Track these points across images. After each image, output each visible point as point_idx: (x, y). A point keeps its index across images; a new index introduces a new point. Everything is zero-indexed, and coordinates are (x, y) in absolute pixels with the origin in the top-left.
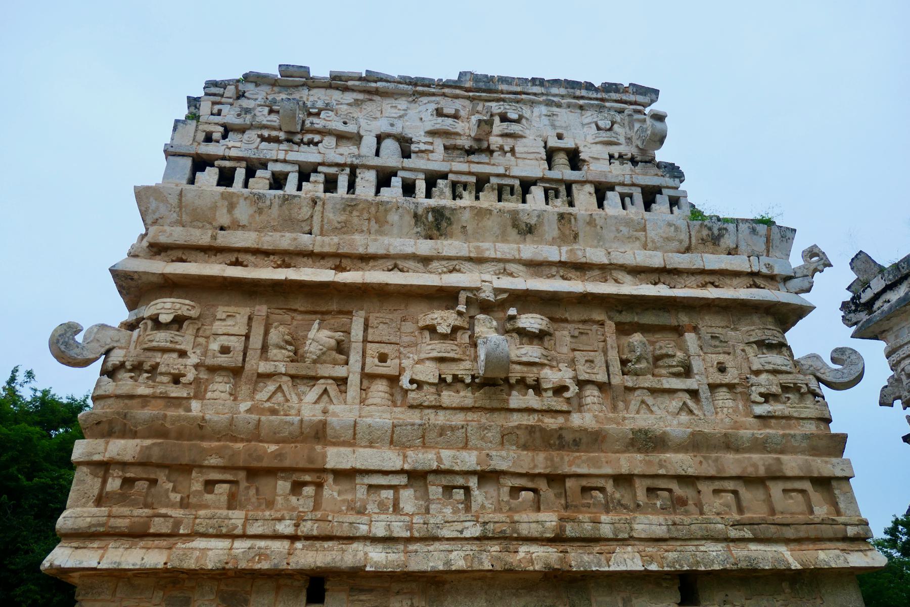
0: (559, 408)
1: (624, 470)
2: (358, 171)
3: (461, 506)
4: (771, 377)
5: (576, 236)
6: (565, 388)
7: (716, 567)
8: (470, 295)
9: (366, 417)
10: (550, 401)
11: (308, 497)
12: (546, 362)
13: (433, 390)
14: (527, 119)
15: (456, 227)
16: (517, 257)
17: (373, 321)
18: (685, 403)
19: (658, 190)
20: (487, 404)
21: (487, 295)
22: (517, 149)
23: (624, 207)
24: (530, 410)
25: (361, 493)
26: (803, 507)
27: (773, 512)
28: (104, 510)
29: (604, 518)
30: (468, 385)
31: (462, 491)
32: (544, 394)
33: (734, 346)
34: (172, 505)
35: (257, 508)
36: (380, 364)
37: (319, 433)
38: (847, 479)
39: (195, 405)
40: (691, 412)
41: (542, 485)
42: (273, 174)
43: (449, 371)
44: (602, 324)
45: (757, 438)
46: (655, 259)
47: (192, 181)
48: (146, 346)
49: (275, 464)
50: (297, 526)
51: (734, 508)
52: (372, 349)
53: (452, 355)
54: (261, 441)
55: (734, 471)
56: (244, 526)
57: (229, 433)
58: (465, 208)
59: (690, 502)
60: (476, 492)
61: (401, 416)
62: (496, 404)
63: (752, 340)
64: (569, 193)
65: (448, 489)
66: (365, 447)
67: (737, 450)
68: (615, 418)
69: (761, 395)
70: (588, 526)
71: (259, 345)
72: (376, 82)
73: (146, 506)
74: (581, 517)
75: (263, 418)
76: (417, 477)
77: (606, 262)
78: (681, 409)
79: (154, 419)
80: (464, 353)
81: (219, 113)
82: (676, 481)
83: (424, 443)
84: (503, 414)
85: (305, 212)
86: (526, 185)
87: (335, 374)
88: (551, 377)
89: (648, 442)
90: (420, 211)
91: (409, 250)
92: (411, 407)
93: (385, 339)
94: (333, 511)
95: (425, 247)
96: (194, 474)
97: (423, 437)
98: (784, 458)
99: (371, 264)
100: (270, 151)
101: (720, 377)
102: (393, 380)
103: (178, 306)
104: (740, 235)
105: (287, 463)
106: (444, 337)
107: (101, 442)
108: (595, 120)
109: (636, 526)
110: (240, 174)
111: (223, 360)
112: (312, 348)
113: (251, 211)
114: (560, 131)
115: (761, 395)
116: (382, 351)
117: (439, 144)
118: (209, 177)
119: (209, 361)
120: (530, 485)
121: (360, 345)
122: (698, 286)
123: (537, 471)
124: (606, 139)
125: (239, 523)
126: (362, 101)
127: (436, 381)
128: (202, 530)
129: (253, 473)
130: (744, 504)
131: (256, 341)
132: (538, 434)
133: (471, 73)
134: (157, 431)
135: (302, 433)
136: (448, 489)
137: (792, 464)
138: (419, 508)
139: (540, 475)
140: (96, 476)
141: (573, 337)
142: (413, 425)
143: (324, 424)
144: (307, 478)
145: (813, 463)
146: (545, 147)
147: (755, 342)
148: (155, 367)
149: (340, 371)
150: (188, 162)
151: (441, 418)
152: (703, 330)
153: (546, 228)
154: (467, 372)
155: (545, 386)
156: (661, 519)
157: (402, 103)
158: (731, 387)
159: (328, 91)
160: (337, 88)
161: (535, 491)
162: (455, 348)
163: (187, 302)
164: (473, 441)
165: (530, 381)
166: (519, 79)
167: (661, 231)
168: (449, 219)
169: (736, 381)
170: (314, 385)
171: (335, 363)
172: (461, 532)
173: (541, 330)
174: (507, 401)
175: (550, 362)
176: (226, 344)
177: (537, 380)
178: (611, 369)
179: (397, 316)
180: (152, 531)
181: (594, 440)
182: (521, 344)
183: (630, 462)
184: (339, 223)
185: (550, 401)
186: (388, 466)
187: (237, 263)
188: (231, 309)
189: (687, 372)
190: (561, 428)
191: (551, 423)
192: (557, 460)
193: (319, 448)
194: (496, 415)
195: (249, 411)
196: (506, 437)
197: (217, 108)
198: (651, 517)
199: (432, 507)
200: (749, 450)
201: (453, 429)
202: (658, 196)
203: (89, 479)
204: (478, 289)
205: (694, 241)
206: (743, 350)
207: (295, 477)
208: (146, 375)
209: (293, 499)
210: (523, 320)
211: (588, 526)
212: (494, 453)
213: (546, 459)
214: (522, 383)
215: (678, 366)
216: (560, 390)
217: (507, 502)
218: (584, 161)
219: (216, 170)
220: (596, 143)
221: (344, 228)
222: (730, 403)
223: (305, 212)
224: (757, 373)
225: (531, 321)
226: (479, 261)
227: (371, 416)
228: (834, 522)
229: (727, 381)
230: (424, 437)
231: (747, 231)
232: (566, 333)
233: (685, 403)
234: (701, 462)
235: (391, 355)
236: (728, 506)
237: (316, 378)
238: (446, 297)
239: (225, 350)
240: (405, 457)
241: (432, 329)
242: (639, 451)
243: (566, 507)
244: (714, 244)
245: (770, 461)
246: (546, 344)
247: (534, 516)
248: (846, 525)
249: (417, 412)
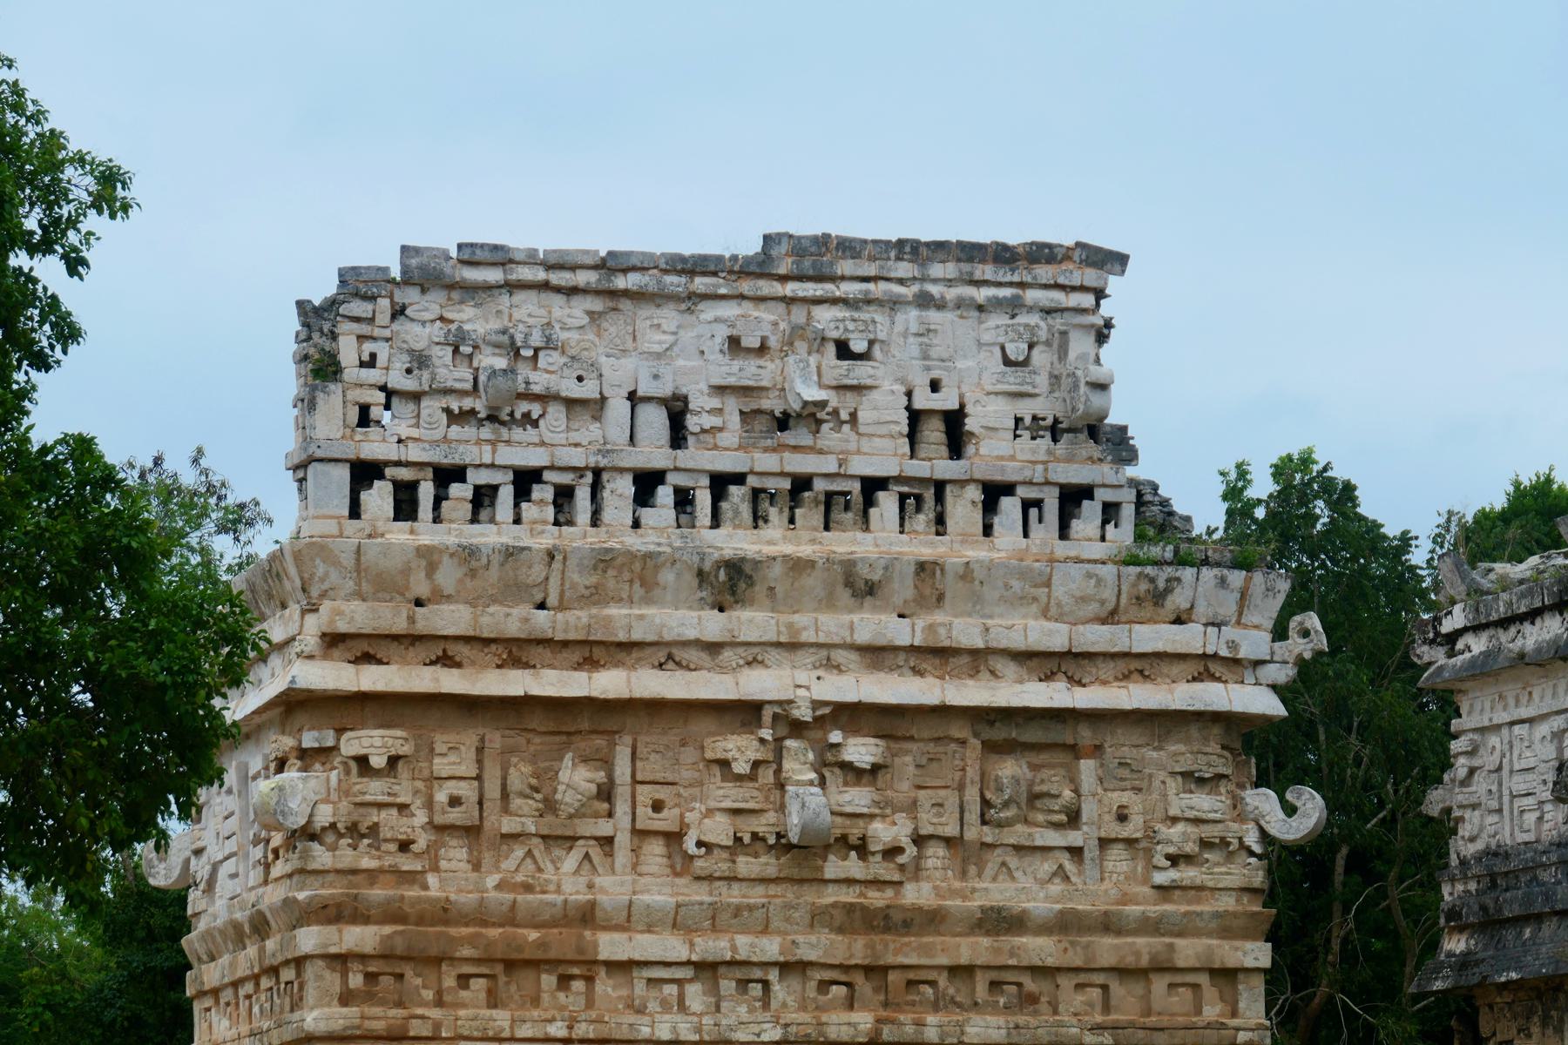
0: (888, 878)
1: (964, 960)
2: (605, 476)
3: (758, 1004)
4: (1190, 829)
5: (940, 598)
6: (898, 850)
8: (778, 710)
9: (642, 892)
10: (879, 868)
11: (578, 994)
12: (877, 811)
13: (725, 855)
14: (882, 342)
15: (760, 590)
16: (848, 640)
17: (641, 749)
18: (1061, 866)
20: (795, 873)
21: (804, 713)
22: (860, 414)
23: (1026, 535)
24: (849, 882)
25: (640, 988)
27: (1148, 1012)
28: (353, 1011)
29: (931, 1019)
30: (771, 847)
31: (759, 986)
32: (871, 858)
33: (1150, 776)
34: (425, 1004)
35: (522, 1007)
36: (655, 815)
37: (587, 916)
39: (432, 879)
40: (1067, 878)
41: (858, 979)
42: (477, 489)
43: (748, 826)
44: (963, 742)
46: (1054, 636)
47: (355, 512)
48: (358, 800)
49: (539, 955)
50: (570, 1028)
51: (1098, 1008)
52: (645, 794)
53: (751, 805)
54: (517, 926)
55: (1107, 960)
56: (512, 1028)
57: (480, 917)
58: (774, 559)
59: (1043, 999)
60: (776, 987)
61: (686, 891)
62: (806, 874)
63: (1178, 770)
64: (939, 498)
65: (743, 984)
66: (642, 932)
67: (1119, 932)
68: (962, 890)
69: (1168, 857)
70: (910, 1029)
71: (497, 794)
72: (625, 271)
73: (400, 1004)
74: (902, 1018)
75: (520, 898)
76: (707, 969)
77: (980, 644)
78: (1054, 874)
79: (389, 901)
80: (767, 798)
81: (371, 362)
83: (713, 925)
84: (815, 887)
85: (538, 572)
86: (873, 486)
87: (600, 834)
88: (883, 832)
89: (1001, 922)
90: (707, 566)
91: (691, 634)
92: (698, 878)
93: (659, 777)
94: (609, 1011)
95: (712, 625)
96: (444, 967)
97: (713, 918)
98: (1180, 943)
99: (635, 654)
100: (468, 445)
101: (1118, 828)
102: (673, 838)
103: (390, 741)
104: (1200, 589)
105: (552, 954)
106: (740, 778)
107: (332, 929)
108: (1001, 339)
109: (968, 1029)
110: (426, 491)
111: (455, 816)
112: (568, 799)
113: (459, 573)
114: (935, 374)
115: (1168, 857)
116: (657, 796)
117: (732, 405)
118: (378, 498)
119: (439, 819)
120: (843, 978)
121: (628, 789)
122: (1117, 679)
123: (853, 962)
124: (1013, 388)
125: (506, 1024)
126: (600, 314)
127: (730, 843)
128: (466, 1033)
129: (511, 965)
130: (1113, 1002)
131: (493, 790)
132: (858, 914)
133: (791, 236)
134: (392, 915)
135: (566, 916)
136: (743, 984)
138: (708, 1007)
139: (856, 966)
140: (334, 970)
141: (918, 766)
142: (701, 903)
143: (593, 905)
144: (576, 971)
146: (908, 408)
147: (1182, 774)
148: (374, 829)
149: (604, 828)
150: (343, 474)
151: (734, 895)
153: (896, 586)
154: (770, 829)
155: (873, 848)
156: (1001, 1021)
157: (669, 316)
158: (1130, 842)
159: (543, 295)
160: (558, 290)
161: (848, 984)
162: (756, 793)
163: (399, 733)
164: (776, 923)
165: (853, 840)
166: (875, 242)
167: (1073, 586)
168: (750, 577)
169: (1138, 835)
170: (571, 848)
171: (596, 815)
172: (758, 1035)
173: (874, 765)
174: (821, 869)
175: (884, 809)
176: (455, 792)
177: (863, 838)
178: (967, 815)
179: (673, 737)
180: (412, 1034)
181: (933, 920)
182: (846, 784)
183: (973, 949)
184: (587, 588)
185: (879, 868)
186: (671, 956)
187: (446, 661)
188: (452, 737)
189: (1073, 818)
190: (888, 907)
191: (877, 899)
192: (879, 947)
193: (587, 933)
194: (806, 887)
195: (498, 887)
196: (818, 918)
197: (368, 347)
198: (988, 1018)
199: (724, 1005)
200: (1136, 932)
201: (751, 908)
202: (1086, 503)
203: (327, 974)
204: (790, 702)
205: (1124, 600)
206: (1164, 782)
207: (561, 970)
208: (366, 841)
209: (561, 996)
210: (851, 749)
211: (910, 1029)
212: (800, 939)
213: (866, 946)
214: (844, 844)
215: (1060, 812)
216: (892, 852)
217: (814, 1000)
218: (972, 434)
219: (389, 487)
220: (997, 394)
221: (596, 596)
222: (1124, 867)
223: (538, 572)
224: (1175, 820)
225: (861, 750)
226: (793, 646)
227: (648, 891)
228: (1223, 1026)
229: (1125, 835)
230: (715, 919)
231: (1213, 582)
232: (908, 759)
234: (1066, 950)
235: (669, 803)
237: (575, 839)
238: (746, 712)
239: (455, 801)
240: (692, 945)
241: (725, 764)
242: (988, 933)
243: (886, 1005)
244: (1156, 604)
245: (1159, 948)
246: (880, 784)
247: (846, 1017)
248: (1238, 1029)
249: (705, 886)
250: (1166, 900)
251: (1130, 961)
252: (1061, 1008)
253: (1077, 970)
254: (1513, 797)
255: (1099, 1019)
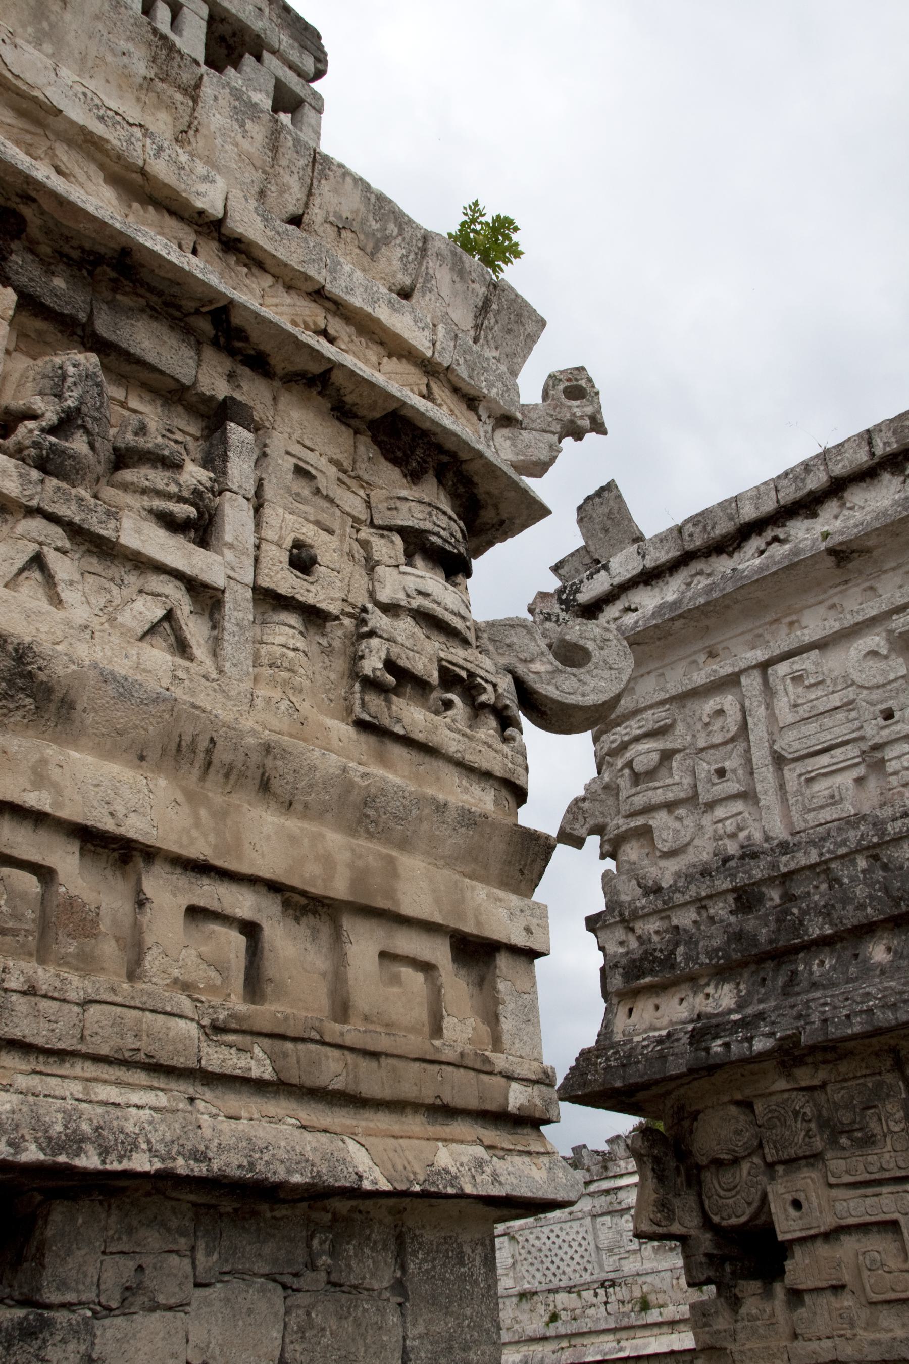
7: (141, 1163)
19: (257, 48)
26: (420, 1014)
27: (342, 1009)
38: (532, 955)
40: (182, 647)
45: (349, 786)
55: (267, 864)
69: (390, 665)
78: (153, 630)
82: (75, 847)
130: (270, 968)
137: (420, 887)
145: (468, 894)
147: (403, 531)
152: (278, 442)
158: (314, 617)
169: (334, 608)
189: (201, 529)
224: (391, 609)
233: (169, 616)
236: (220, 968)
248: (510, 1077)
250: (382, 760)
251: (309, 877)
252: (152, 962)
253: (201, 868)
254: (779, 761)
255: (238, 1005)
